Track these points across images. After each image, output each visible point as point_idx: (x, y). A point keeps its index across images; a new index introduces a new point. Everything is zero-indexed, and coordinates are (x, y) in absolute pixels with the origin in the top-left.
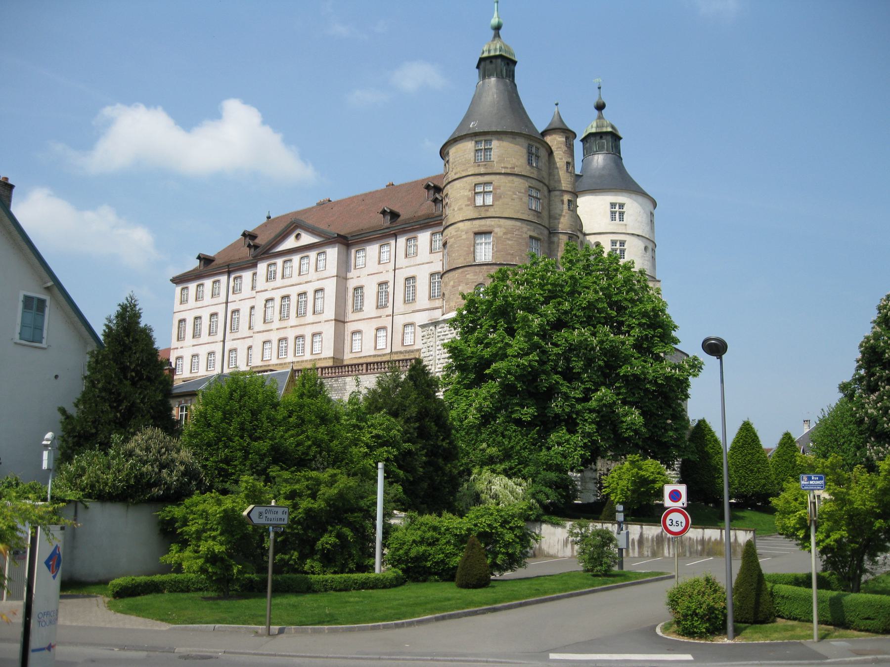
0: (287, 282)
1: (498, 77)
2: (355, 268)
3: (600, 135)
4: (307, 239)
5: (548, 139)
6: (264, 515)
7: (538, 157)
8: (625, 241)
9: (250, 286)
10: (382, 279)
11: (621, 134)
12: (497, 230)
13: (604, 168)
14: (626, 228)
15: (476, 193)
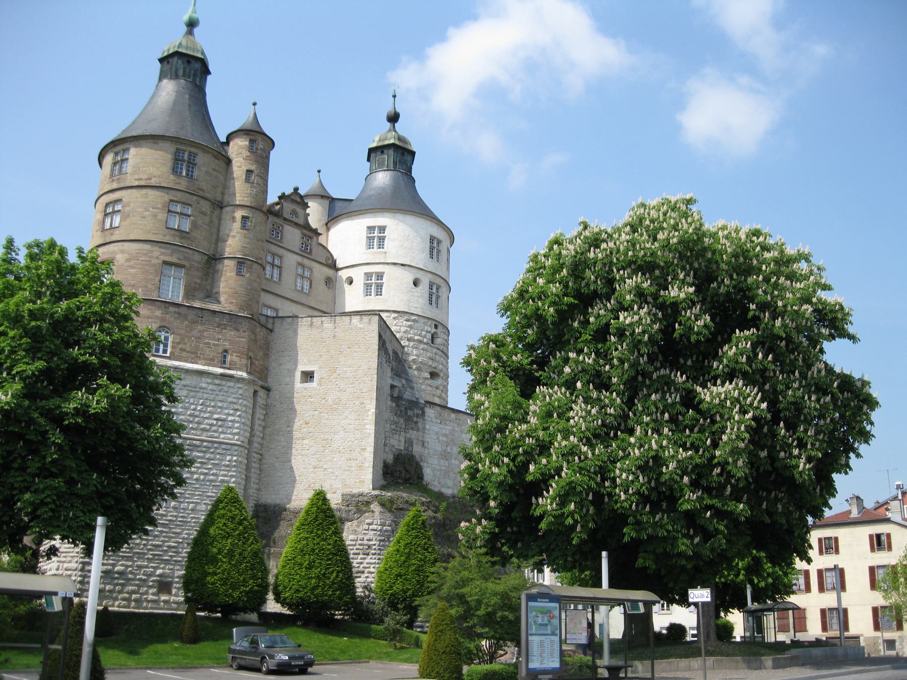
8: (384, 273)
14: (385, 257)
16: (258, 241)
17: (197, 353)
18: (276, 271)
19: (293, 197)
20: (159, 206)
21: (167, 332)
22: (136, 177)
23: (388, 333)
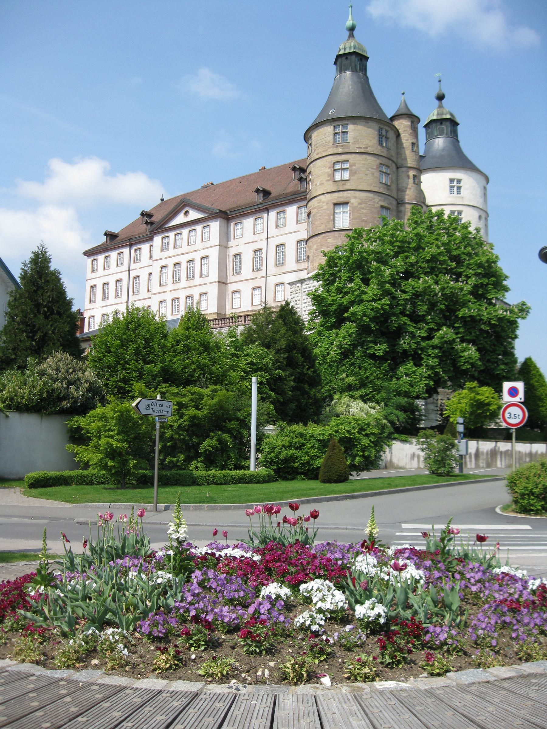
0: (178, 251)
1: (352, 71)
2: (234, 239)
3: (440, 121)
4: (194, 215)
5: (396, 123)
6: (151, 407)
7: (387, 138)
9: (148, 256)
10: (257, 246)
11: (458, 120)
12: (353, 201)
13: (443, 149)
15: (335, 170)
20: (375, 167)
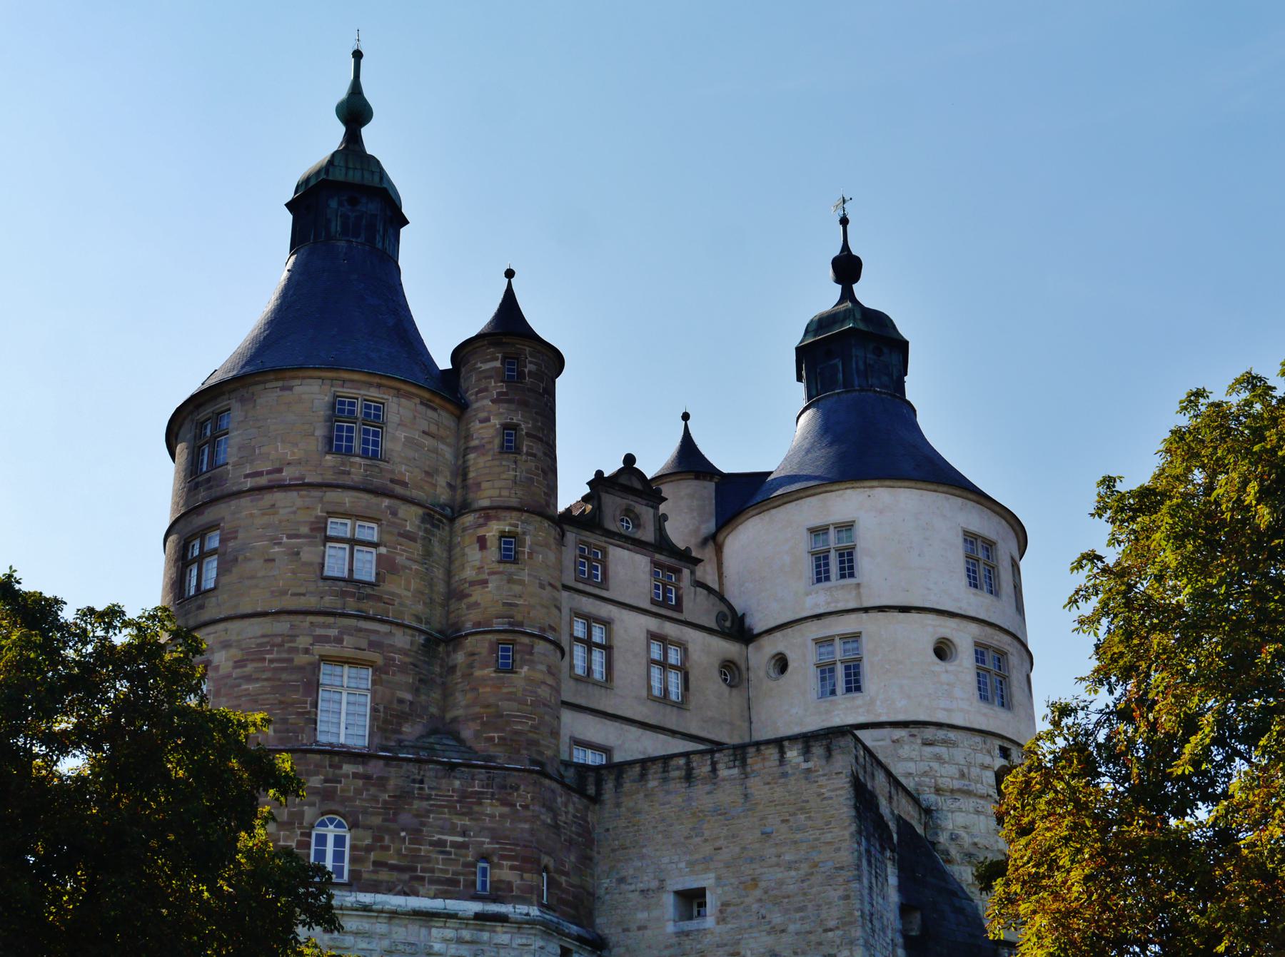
14: (859, 596)
16: (542, 586)
17: (414, 869)
18: (598, 656)
19: (623, 480)
20: (305, 530)
21: (339, 825)
22: (248, 472)
23: (881, 778)
